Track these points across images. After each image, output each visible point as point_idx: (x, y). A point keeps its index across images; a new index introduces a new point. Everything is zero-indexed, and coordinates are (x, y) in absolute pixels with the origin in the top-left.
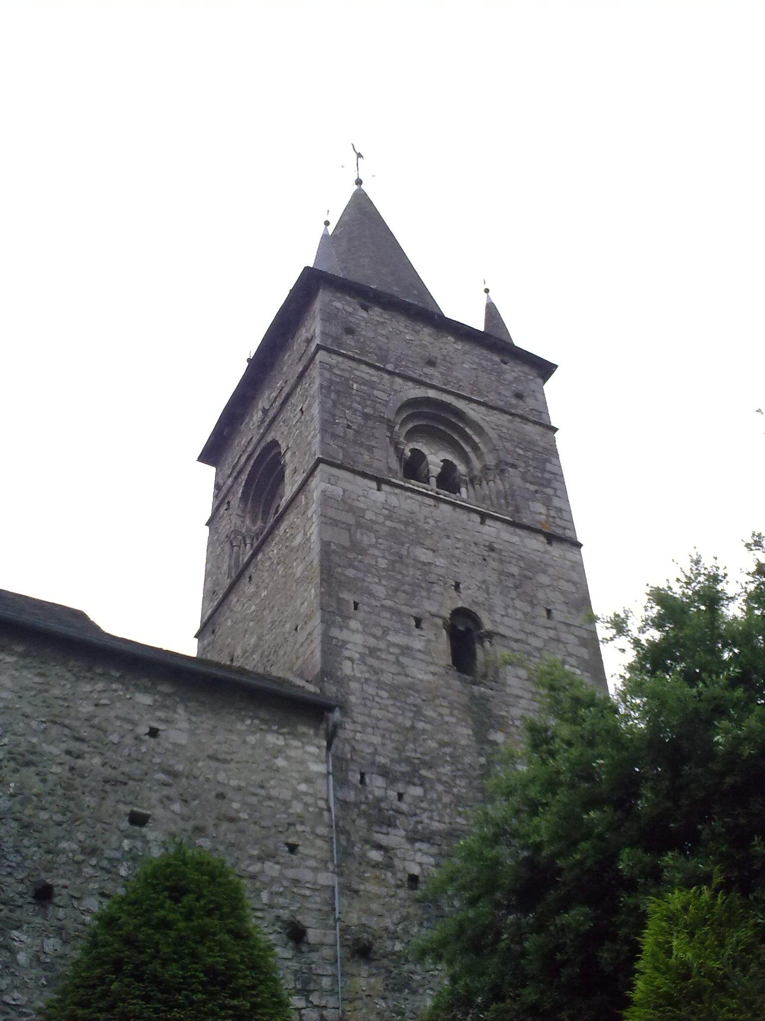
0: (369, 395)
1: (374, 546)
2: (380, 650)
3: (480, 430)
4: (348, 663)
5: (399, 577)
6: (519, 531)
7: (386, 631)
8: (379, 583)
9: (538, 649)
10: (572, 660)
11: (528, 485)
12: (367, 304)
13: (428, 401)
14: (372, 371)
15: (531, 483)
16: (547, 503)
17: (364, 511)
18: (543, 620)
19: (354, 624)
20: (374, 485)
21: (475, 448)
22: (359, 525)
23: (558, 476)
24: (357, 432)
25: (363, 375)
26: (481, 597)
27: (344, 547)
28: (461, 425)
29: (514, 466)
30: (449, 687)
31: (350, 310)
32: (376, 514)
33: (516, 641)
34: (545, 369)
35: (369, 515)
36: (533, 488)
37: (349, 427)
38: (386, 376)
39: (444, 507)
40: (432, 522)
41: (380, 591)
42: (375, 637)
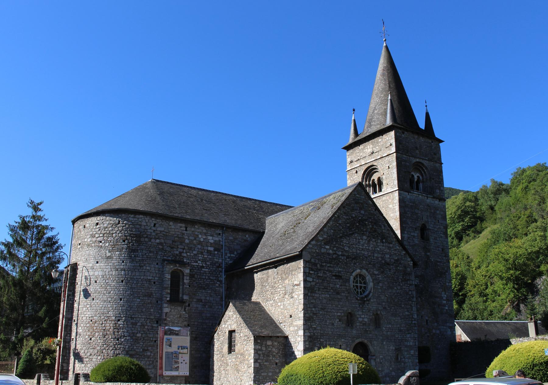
3: (426, 168)
13: (417, 162)
14: (406, 156)
16: (440, 189)
20: (407, 194)
21: (425, 172)
23: (442, 179)
26: (426, 220)
29: (433, 179)
34: (441, 141)
39: (420, 196)
41: (410, 223)
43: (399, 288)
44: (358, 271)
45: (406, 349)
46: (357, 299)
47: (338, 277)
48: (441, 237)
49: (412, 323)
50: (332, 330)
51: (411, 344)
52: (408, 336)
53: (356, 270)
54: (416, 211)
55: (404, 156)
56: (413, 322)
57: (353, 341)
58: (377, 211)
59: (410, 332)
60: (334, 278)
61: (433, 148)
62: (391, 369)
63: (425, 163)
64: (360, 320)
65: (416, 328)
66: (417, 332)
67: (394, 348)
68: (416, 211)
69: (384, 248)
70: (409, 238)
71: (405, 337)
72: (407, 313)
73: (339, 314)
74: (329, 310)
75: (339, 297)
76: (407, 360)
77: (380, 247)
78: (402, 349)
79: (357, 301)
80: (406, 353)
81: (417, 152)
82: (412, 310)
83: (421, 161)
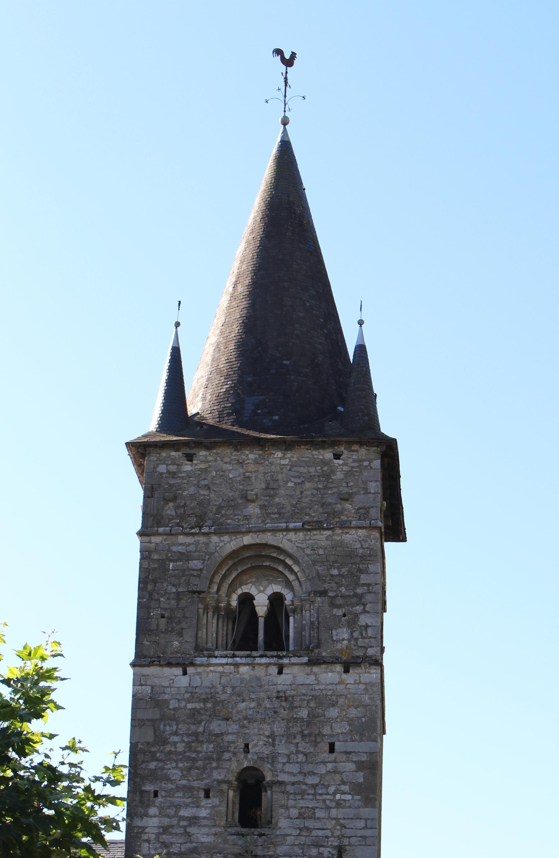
0: (184, 571)
1: (176, 734)
2: (172, 826)
4: (146, 845)
5: (194, 755)
6: (316, 669)
7: (178, 807)
8: (177, 767)
9: (314, 786)
10: (345, 788)
11: (335, 610)
12: (192, 452)
15: (339, 607)
16: (352, 624)
17: (167, 702)
18: (326, 756)
19: (153, 811)
20: (179, 671)
22: (163, 718)
24: (171, 619)
25: (180, 549)
27: (148, 743)
28: (282, 557)
30: (226, 841)
31: (173, 468)
32: (179, 701)
33: (293, 784)
35: (173, 704)
36: (340, 612)
37: (163, 617)
38: (202, 539)
40: (229, 691)
41: (175, 774)
42: (169, 816)
48: (339, 804)
54: (216, 726)
55: (182, 539)
61: (339, 475)
63: (286, 545)
68: (216, 726)
70: (165, 829)
81: (253, 509)
83: (269, 538)
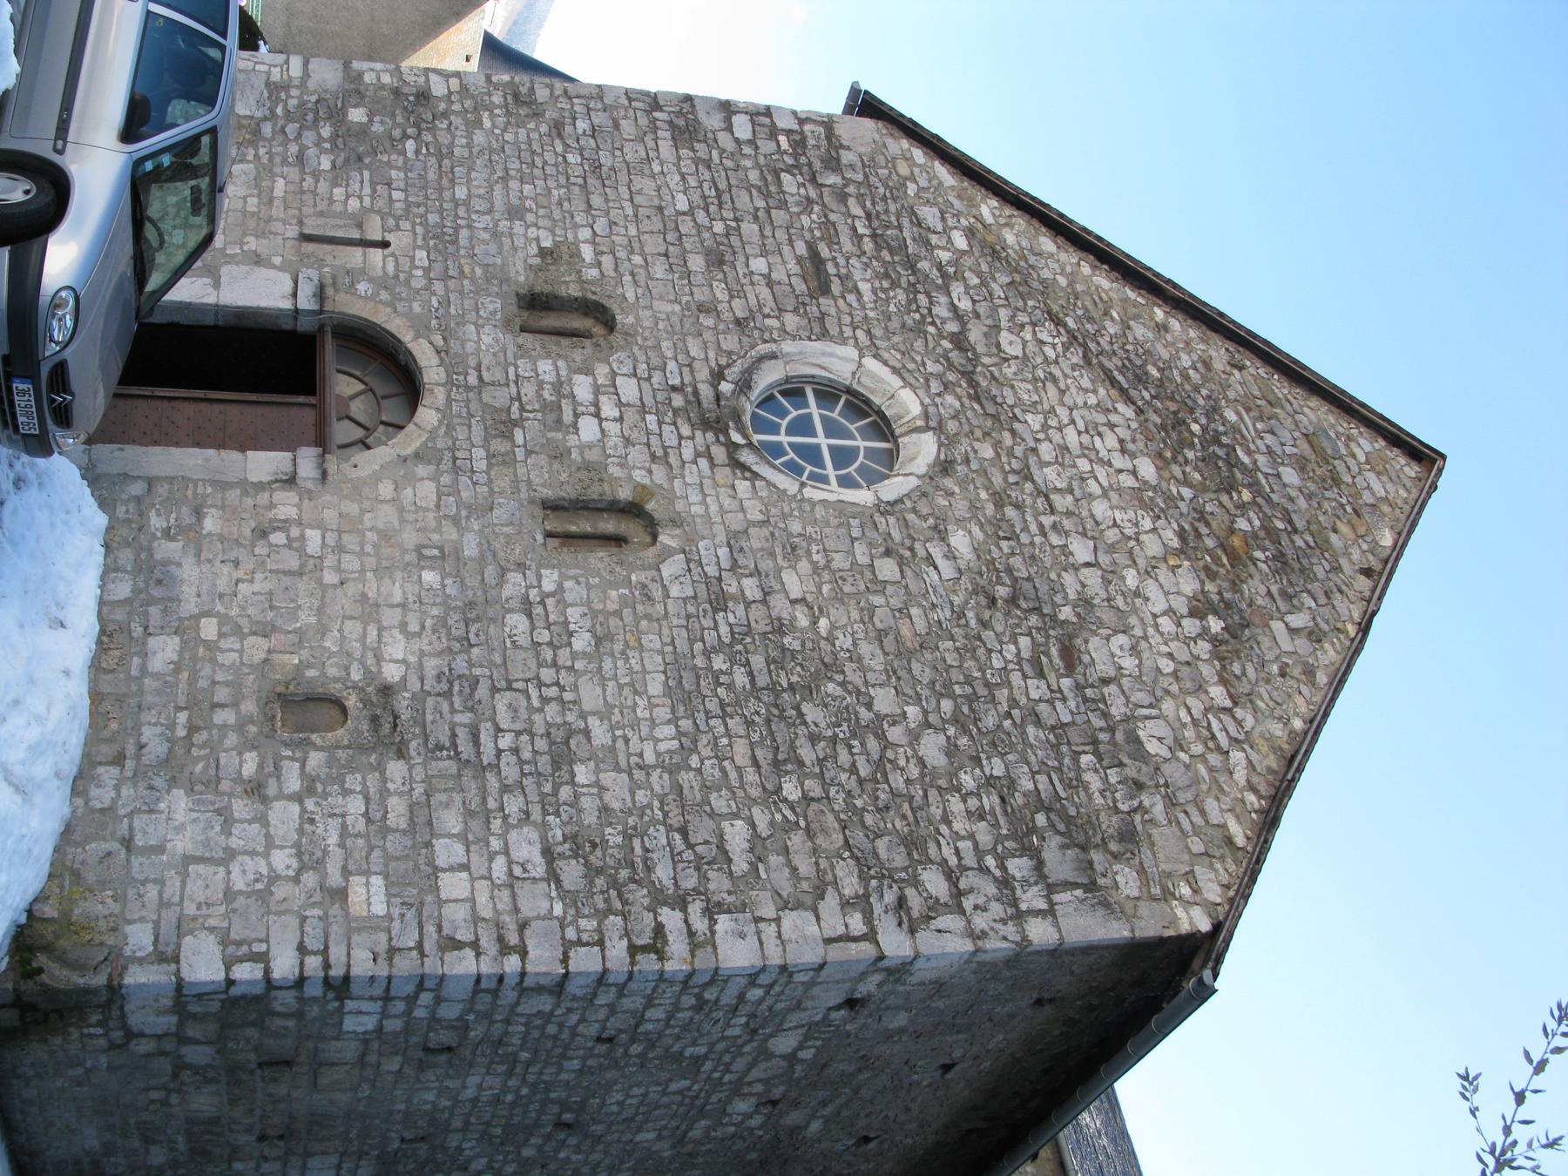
43: (932, 747)
44: (907, 404)
45: (397, 811)
46: (718, 376)
47: (816, 270)
49: (659, 899)
50: (479, 205)
51: (454, 885)
52: (526, 847)
53: (907, 384)
56: (671, 918)
57: (422, 330)
58: (1364, 584)
59: (572, 873)
60: (801, 248)
62: (209, 628)
64: (582, 388)
65: (617, 950)
66: (585, 961)
67: (392, 673)
69: (1166, 624)
71: (513, 805)
72: (737, 835)
73: (587, 252)
74: (597, 201)
75: (697, 263)
76: (285, 816)
77: (1151, 589)
78: (396, 769)
79: (703, 374)
80: (356, 806)
82: (785, 905)
